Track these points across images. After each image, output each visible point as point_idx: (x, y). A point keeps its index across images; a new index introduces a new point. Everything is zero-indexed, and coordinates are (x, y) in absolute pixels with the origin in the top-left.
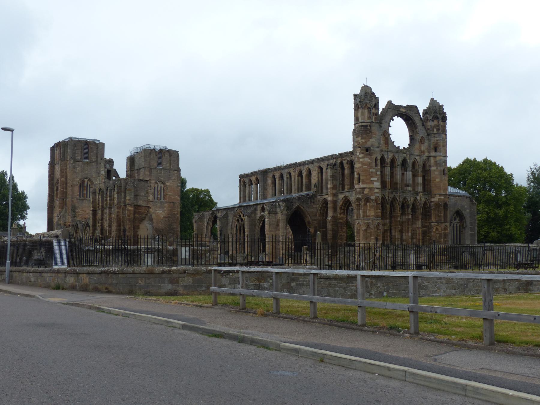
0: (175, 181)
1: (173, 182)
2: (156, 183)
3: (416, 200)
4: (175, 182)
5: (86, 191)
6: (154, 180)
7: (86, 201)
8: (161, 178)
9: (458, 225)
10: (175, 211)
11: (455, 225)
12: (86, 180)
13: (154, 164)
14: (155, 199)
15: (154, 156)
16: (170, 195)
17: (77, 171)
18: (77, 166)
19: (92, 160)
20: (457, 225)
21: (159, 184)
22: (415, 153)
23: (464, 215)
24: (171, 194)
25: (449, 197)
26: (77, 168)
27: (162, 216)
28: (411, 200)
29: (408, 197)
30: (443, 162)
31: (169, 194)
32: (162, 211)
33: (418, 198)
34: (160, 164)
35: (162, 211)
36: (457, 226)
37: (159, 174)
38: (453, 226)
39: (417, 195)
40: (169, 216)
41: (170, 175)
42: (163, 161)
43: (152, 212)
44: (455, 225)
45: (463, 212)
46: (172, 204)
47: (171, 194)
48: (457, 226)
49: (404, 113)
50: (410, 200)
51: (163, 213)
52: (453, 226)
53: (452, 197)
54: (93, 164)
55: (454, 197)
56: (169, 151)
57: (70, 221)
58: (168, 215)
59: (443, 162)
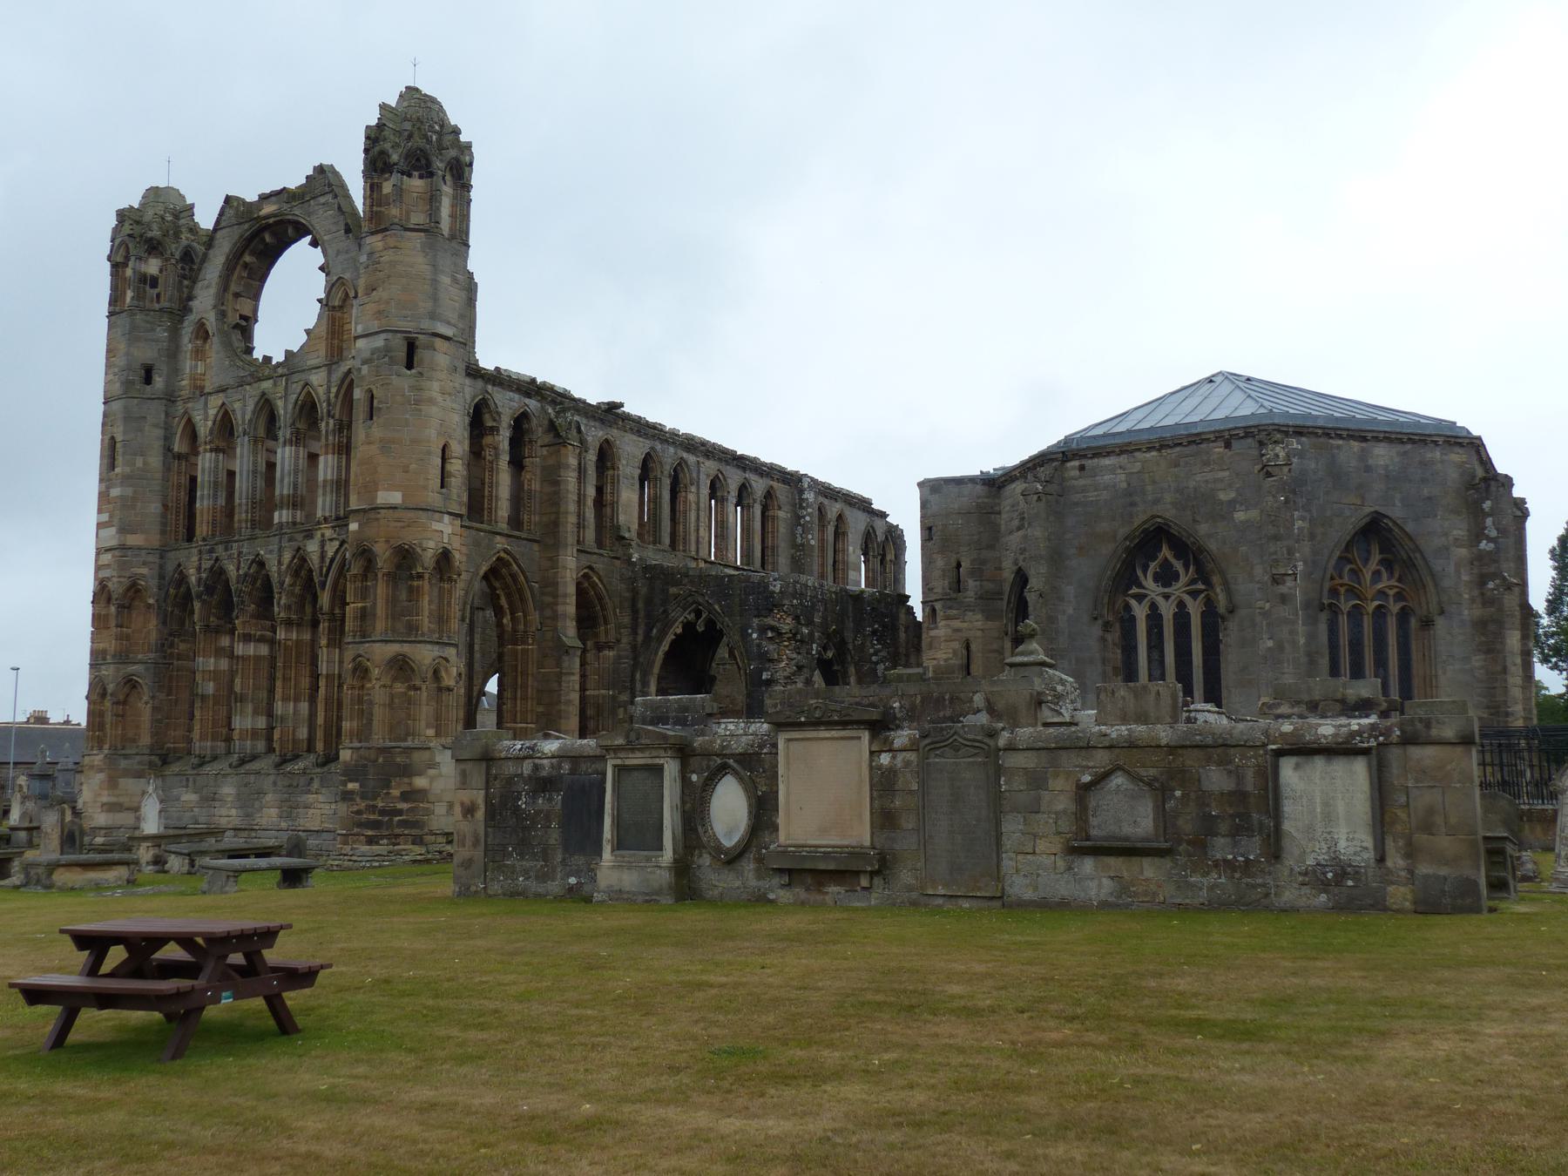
3: (301, 559)
9: (1195, 609)
11: (1167, 610)
20: (1181, 605)
22: (309, 363)
23: (1213, 546)
25: (1088, 463)
28: (278, 561)
29: (271, 552)
30: (365, 362)
33: (312, 547)
36: (1182, 618)
38: (1155, 617)
39: (309, 535)
44: (1167, 610)
45: (1203, 528)
48: (1182, 618)
49: (271, 221)
50: (280, 563)
52: (1155, 617)
53: (1107, 461)
55: (1123, 459)
59: (365, 362)
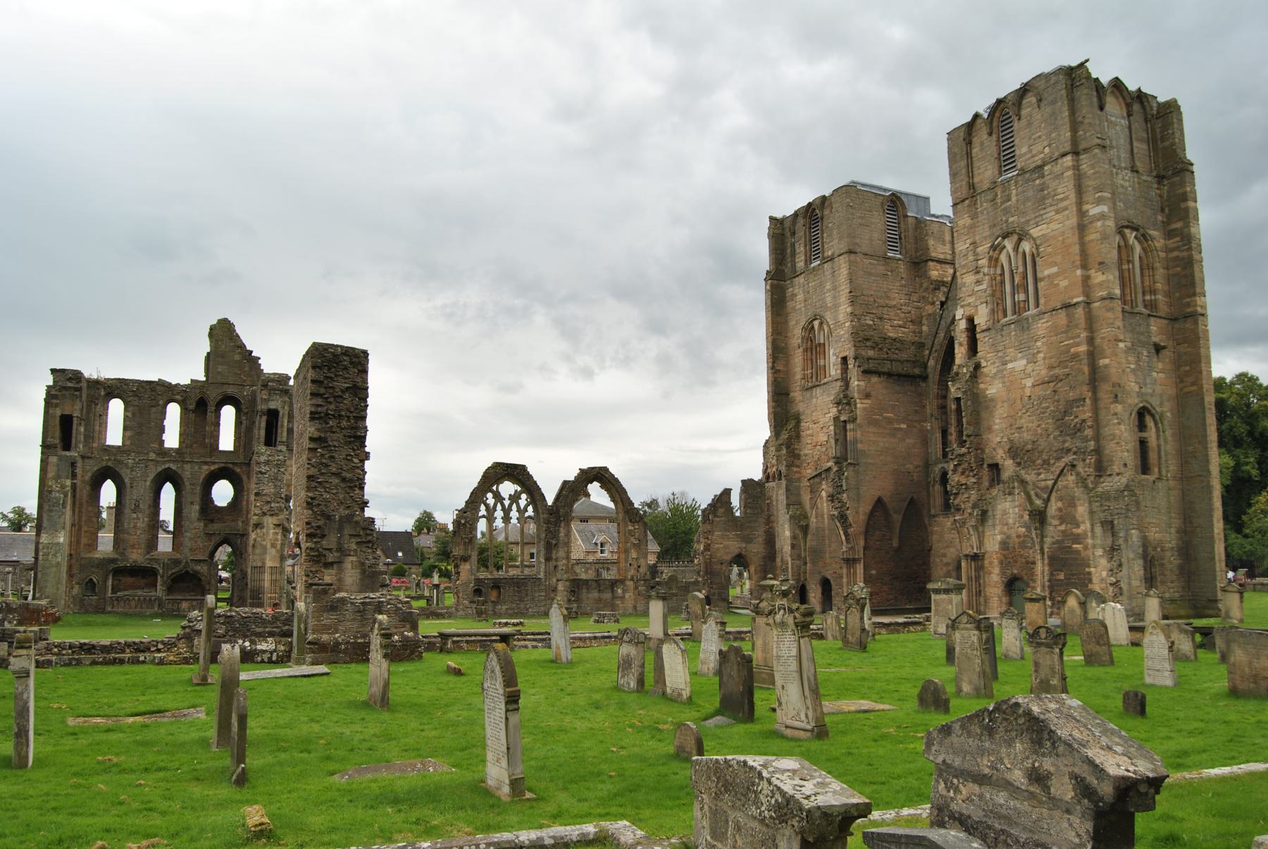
0: (1065, 203)
1: (1057, 212)
2: (994, 248)
4: (1066, 209)
5: (822, 356)
6: (985, 238)
7: (818, 389)
8: (1011, 220)
10: (1078, 345)
12: (816, 323)
13: (986, 172)
14: (1005, 316)
15: (982, 144)
16: (1049, 276)
17: (798, 307)
18: (796, 291)
19: (826, 254)
21: (1009, 245)
24: (1055, 269)
26: (796, 295)
27: (1029, 383)
31: (1046, 273)
32: (1024, 362)
34: (1006, 158)
35: (1024, 362)
37: (1002, 203)
40: (1057, 371)
41: (1042, 190)
42: (1016, 142)
43: (994, 371)
46: (1063, 314)
47: (1055, 269)
51: (1030, 368)
54: (826, 265)
56: (1024, 90)
57: (774, 462)
58: (1051, 368)
